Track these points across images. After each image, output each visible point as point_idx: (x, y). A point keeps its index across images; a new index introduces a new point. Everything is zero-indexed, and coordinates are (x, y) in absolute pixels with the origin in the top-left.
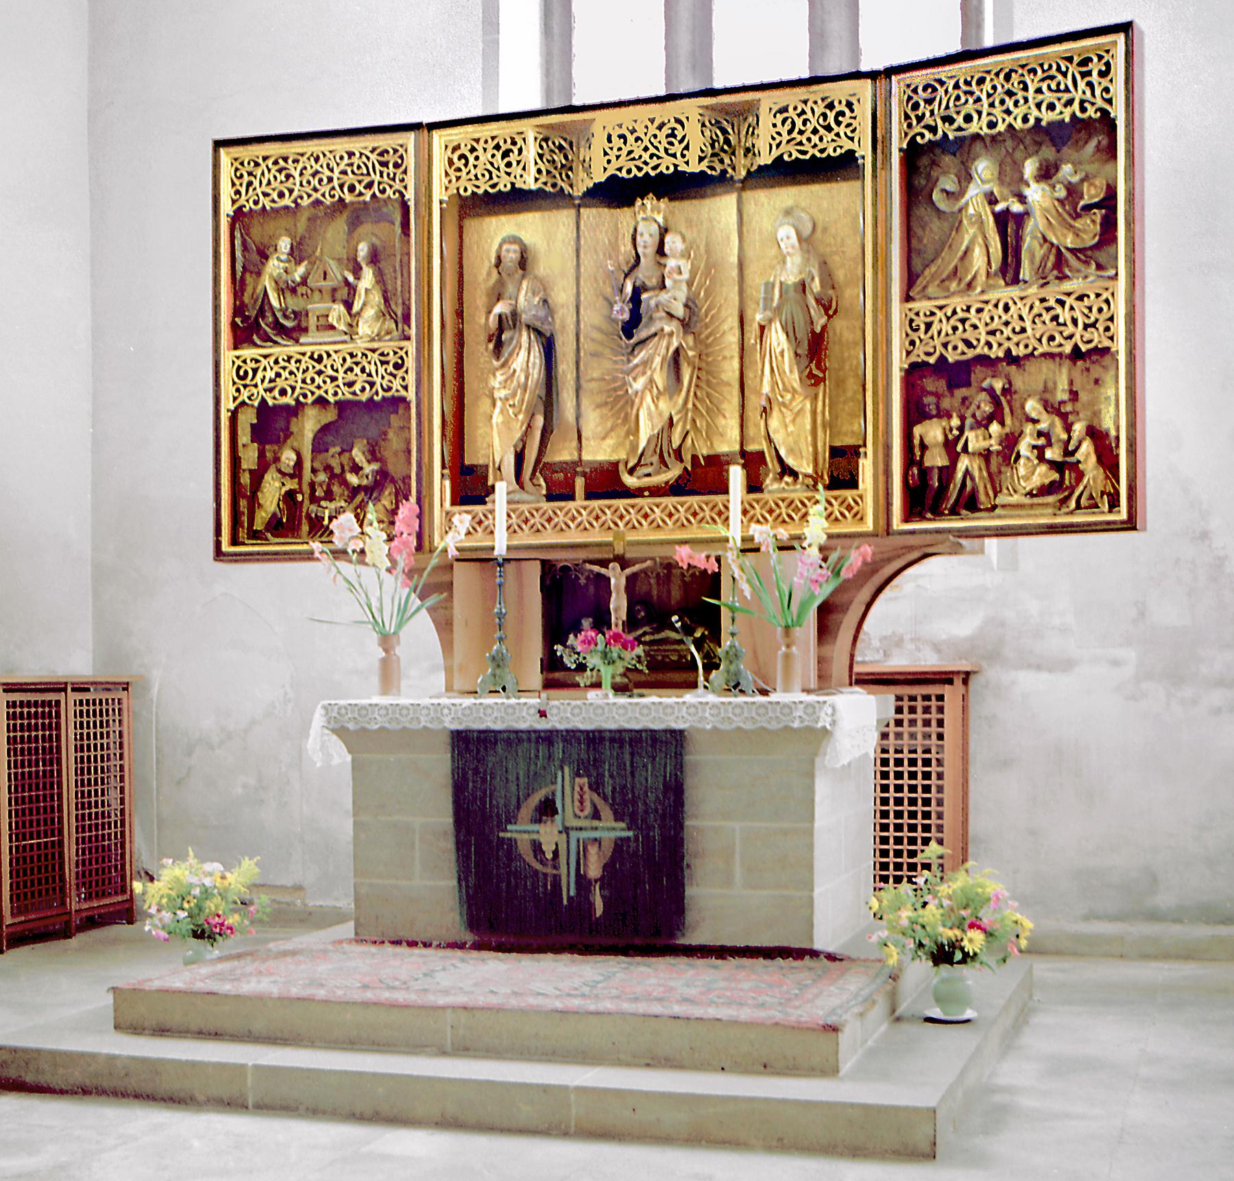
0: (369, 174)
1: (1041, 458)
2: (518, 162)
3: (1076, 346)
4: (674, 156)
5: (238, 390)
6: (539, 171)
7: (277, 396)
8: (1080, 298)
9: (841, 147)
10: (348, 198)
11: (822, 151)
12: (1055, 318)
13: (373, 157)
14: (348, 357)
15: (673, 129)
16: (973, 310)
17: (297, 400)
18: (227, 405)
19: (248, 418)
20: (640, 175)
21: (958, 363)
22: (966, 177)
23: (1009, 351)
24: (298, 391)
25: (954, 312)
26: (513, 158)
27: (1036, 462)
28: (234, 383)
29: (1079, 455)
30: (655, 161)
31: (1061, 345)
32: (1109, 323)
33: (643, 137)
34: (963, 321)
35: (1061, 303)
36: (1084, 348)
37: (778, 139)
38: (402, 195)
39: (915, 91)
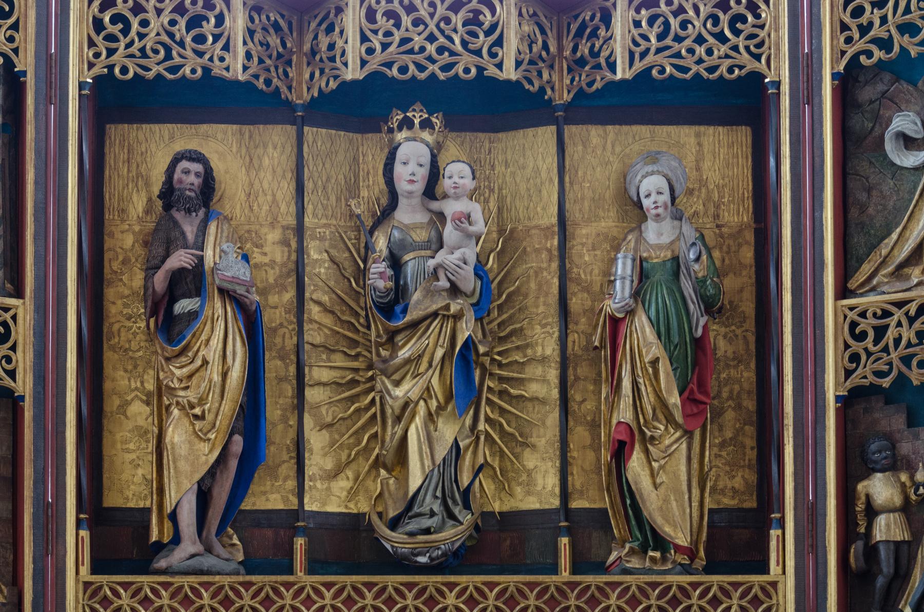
2: (216, 38)
4: (478, 53)
6: (248, 55)
9: (741, 68)
11: (712, 69)
15: (477, 13)
20: (422, 76)
26: (209, 27)
30: (446, 58)
33: (428, 19)
37: (644, 44)
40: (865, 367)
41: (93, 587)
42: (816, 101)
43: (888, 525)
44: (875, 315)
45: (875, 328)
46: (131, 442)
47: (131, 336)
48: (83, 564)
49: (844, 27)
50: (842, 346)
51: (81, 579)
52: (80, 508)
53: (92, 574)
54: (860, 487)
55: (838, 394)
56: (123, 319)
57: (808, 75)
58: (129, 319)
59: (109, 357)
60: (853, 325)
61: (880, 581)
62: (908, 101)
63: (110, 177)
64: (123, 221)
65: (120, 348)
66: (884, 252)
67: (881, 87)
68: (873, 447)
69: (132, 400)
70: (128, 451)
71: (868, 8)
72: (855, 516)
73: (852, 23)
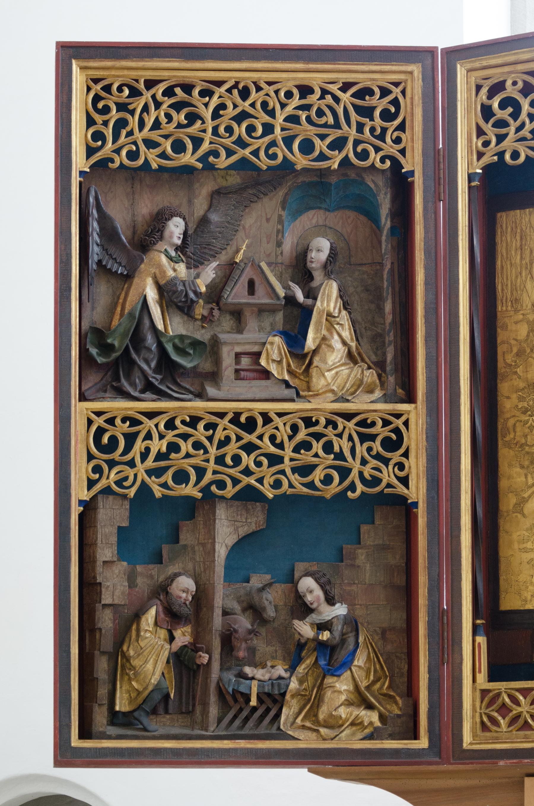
0: (337, 125)
5: (97, 469)
7: (170, 482)
10: (301, 161)
13: (346, 97)
14: (301, 424)
17: (206, 490)
18: (79, 492)
19: (112, 518)
24: (209, 477)
28: (90, 457)
38: (396, 165)
41: (491, 694)
46: (528, 540)
47: (527, 430)
48: (480, 672)
51: (479, 687)
52: (476, 614)
53: (489, 681)
56: (518, 413)
58: (525, 412)
59: (505, 455)
63: (502, 267)
64: (516, 311)
65: (516, 444)
69: (529, 497)
70: (526, 551)
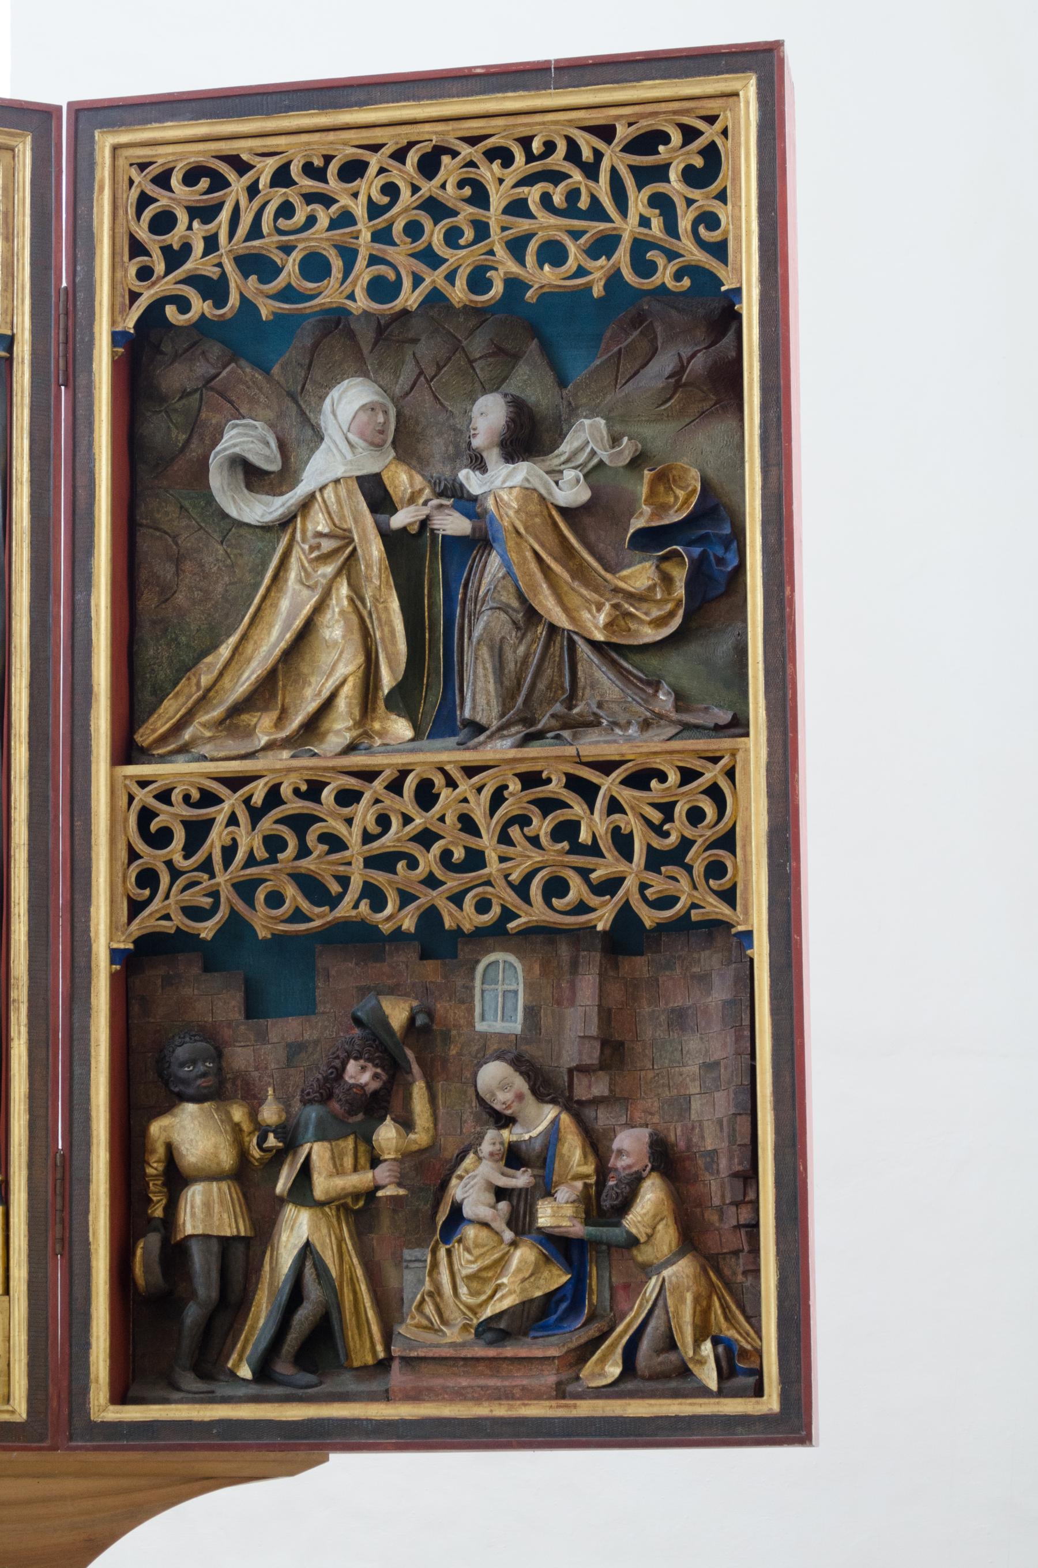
1: (521, 1222)
3: (626, 912)
8: (639, 780)
12: (566, 831)
16: (328, 795)
21: (279, 940)
22: (299, 437)
23: (430, 917)
25: (274, 798)
27: (508, 1235)
29: (636, 1220)
31: (582, 908)
32: (722, 854)
34: (300, 823)
35: (587, 792)
36: (649, 917)
39: (163, 180)
40: (167, 897)
42: (81, 380)
43: (207, 1205)
44: (186, 798)
45: (187, 824)
49: (137, 249)
50: (123, 855)
54: (155, 1128)
55: (115, 946)
57: (66, 330)
60: (146, 815)
61: (192, 1314)
62: (253, 401)
66: (205, 680)
67: (202, 368)
68: (182, 1052)
71: (182, 217)
72: (146, 1185)
73: (153, 243)
